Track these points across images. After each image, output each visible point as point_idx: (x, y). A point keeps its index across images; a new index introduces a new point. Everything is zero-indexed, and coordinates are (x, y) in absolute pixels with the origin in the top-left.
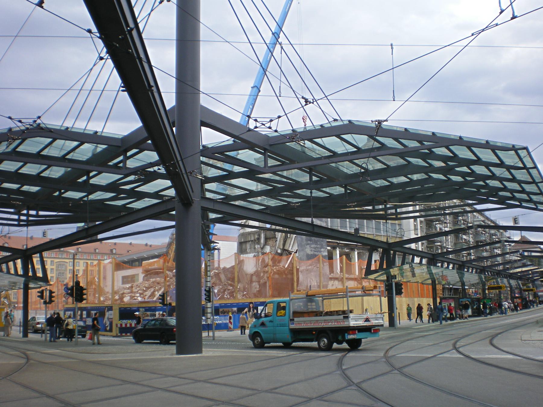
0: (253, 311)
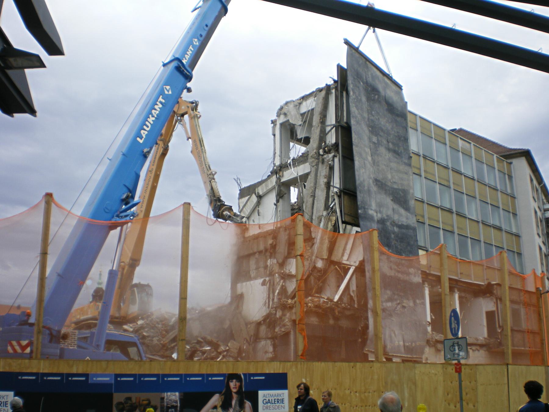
0: (241, 405)
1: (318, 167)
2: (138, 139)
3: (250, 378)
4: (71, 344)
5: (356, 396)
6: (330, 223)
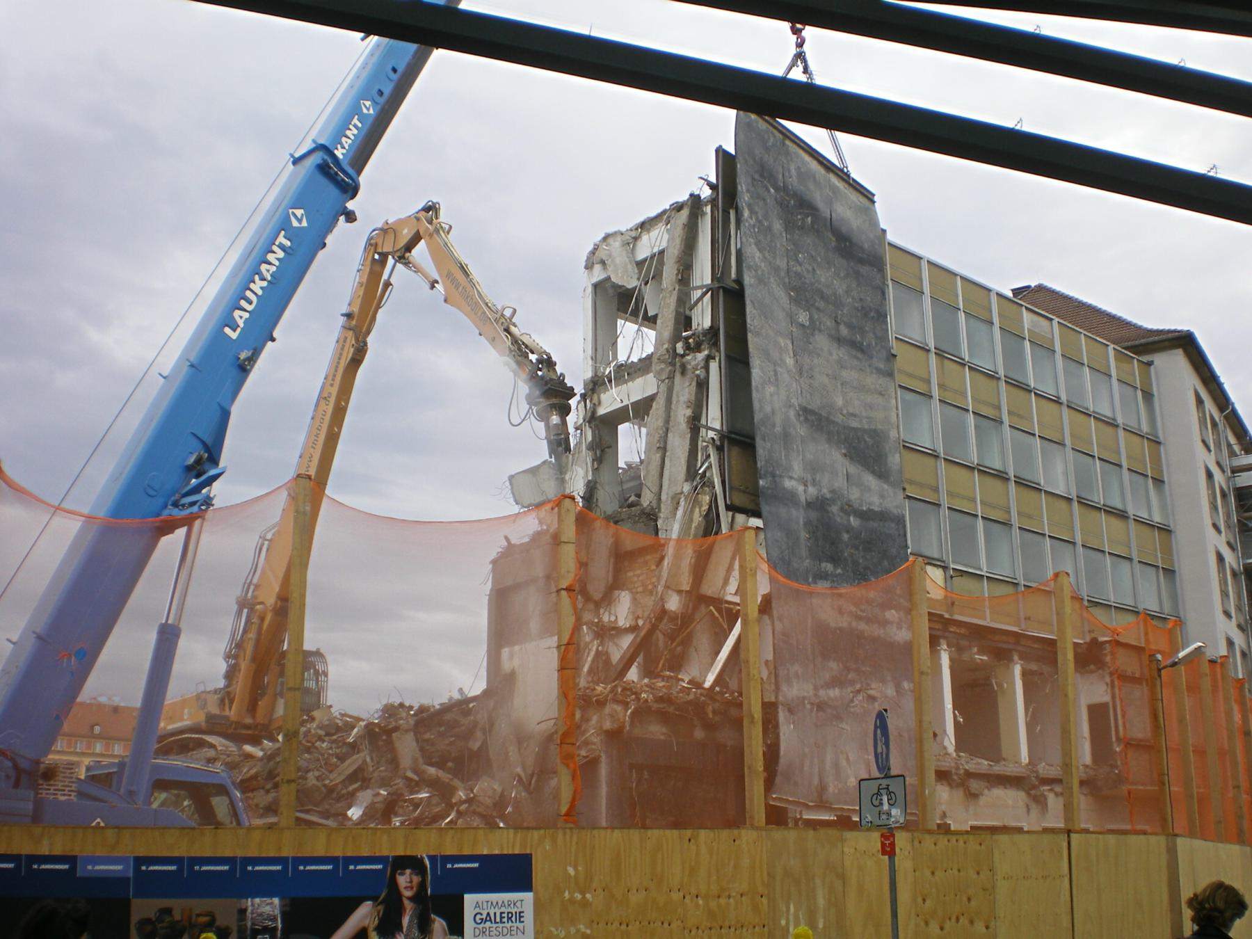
0: (424, 925)
1: (673, 382)
2: (227, 330)
3: (444, 866)
4: (64, 790)
5: (697, 905)
6: (697, 510)
